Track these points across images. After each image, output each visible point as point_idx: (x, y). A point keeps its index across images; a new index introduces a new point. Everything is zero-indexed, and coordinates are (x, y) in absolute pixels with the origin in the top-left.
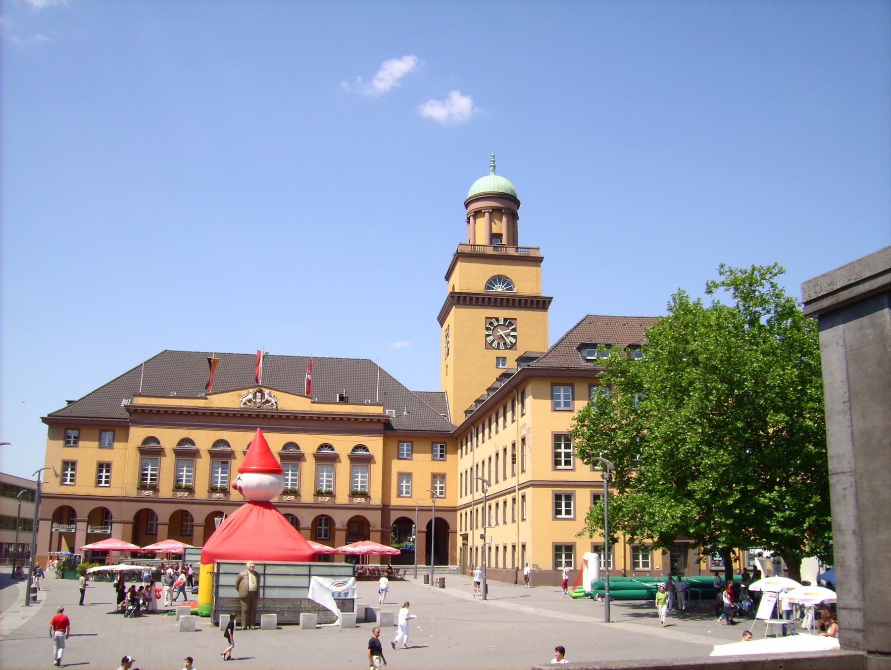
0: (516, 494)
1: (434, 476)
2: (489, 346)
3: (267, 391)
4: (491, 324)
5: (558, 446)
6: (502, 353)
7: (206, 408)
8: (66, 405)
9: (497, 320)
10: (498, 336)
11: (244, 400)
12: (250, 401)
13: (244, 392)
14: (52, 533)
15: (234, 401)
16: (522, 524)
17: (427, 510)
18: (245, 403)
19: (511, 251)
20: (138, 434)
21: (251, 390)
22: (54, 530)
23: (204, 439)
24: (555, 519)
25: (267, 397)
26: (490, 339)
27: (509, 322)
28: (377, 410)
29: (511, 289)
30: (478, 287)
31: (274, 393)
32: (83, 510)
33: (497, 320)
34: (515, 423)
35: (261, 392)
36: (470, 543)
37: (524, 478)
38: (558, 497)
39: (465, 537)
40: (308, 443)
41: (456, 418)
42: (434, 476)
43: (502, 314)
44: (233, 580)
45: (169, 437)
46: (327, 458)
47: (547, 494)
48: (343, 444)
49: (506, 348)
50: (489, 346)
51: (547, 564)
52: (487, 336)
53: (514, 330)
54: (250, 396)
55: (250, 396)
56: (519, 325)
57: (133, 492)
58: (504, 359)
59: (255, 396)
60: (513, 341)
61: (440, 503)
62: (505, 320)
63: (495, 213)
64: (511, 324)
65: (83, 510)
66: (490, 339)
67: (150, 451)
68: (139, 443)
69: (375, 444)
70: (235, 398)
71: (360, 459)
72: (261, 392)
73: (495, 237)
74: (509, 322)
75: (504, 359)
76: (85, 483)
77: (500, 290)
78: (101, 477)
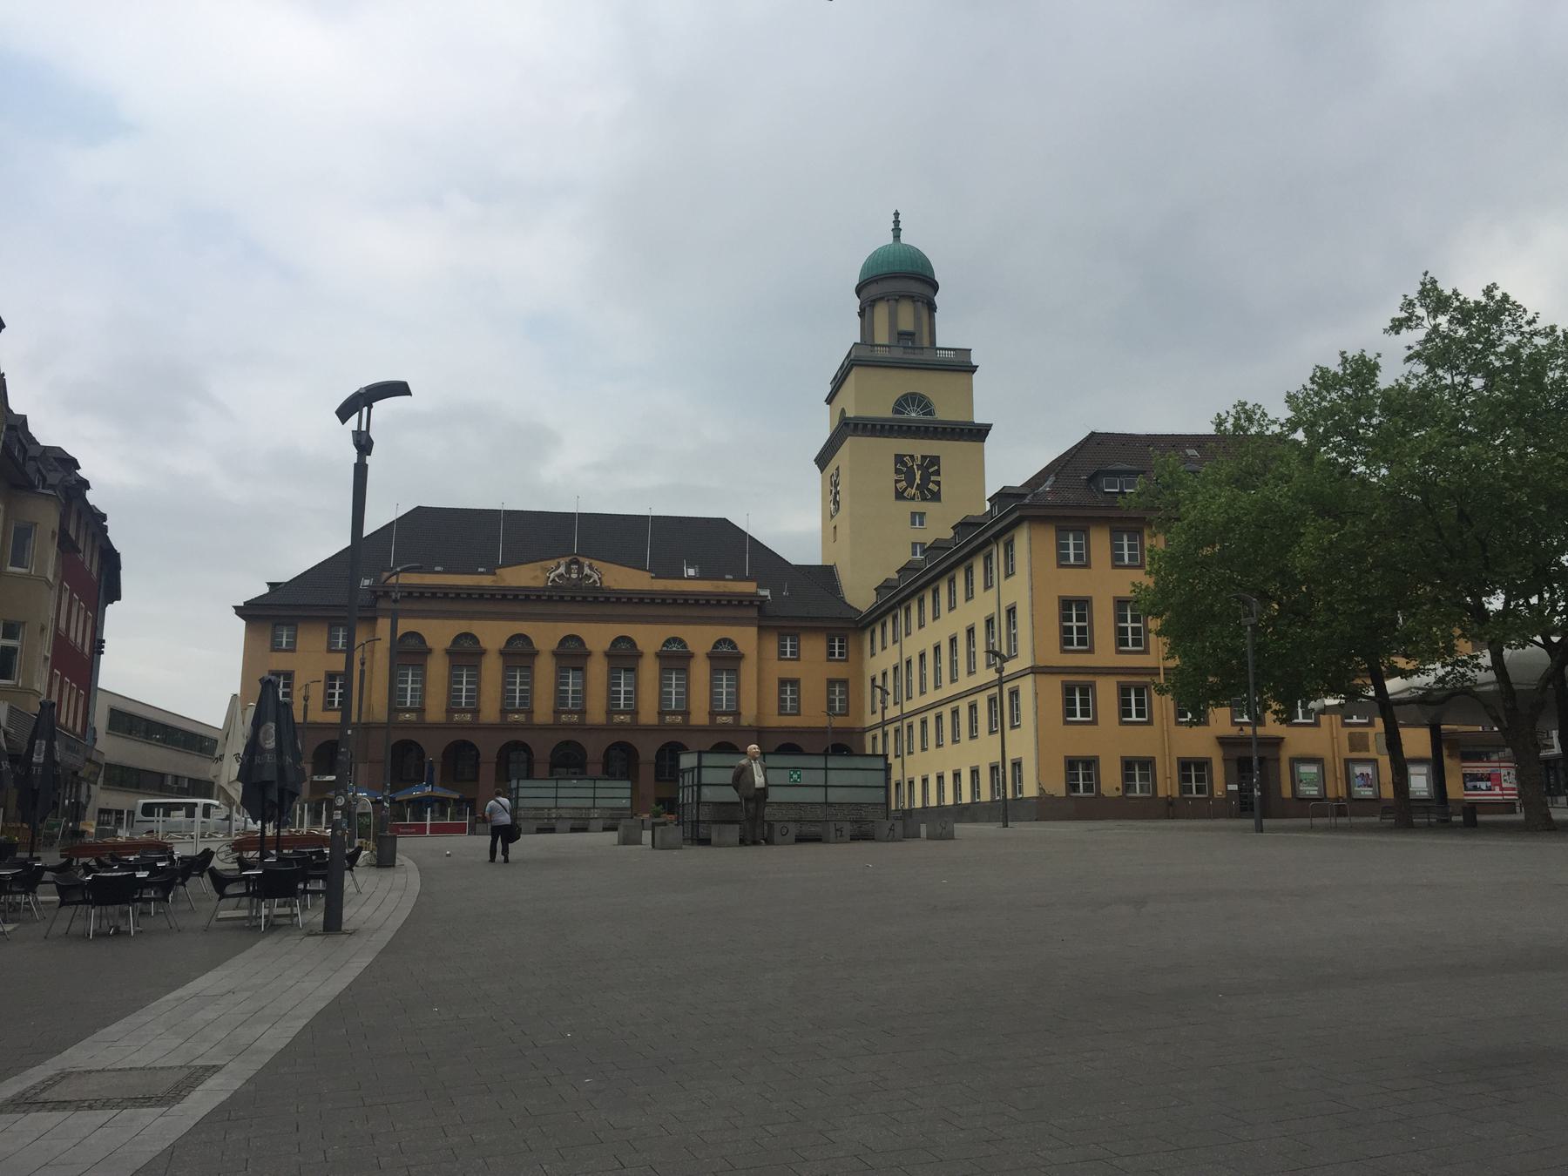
2: (900, 495)
6: (919, 506)
8: (266, 590)
10: (919, 481)
12: (560, 576)
13: (552, 563)
15: (536, 577)
17: (822, 731)
21: (562, 561)
24: (1067, 723)
25: (587, 571)
27: (931, 464)
28: (749, 587)
29: (931, 413)
31: (596, 564)
33: (912, 457)
35: (577, 562)
36: (896, 775)
38: (1068, 690)
40: (649, 637)
45: (439, 633)
46: (675, 659)
47: (1055, 684)
48: (700, 638)
49: (924, 499)
50: (900, 495)
51: (1058, 788)
54: (562, 570)
55: (562, 570)
58: (922, 515)
59: (568, 570)
61: (839, 722)
67: (410, 653)
69: (745, 637)
70: (539, 573)
72: (577, 562)
75: (922, 515)
78: (333, 695)
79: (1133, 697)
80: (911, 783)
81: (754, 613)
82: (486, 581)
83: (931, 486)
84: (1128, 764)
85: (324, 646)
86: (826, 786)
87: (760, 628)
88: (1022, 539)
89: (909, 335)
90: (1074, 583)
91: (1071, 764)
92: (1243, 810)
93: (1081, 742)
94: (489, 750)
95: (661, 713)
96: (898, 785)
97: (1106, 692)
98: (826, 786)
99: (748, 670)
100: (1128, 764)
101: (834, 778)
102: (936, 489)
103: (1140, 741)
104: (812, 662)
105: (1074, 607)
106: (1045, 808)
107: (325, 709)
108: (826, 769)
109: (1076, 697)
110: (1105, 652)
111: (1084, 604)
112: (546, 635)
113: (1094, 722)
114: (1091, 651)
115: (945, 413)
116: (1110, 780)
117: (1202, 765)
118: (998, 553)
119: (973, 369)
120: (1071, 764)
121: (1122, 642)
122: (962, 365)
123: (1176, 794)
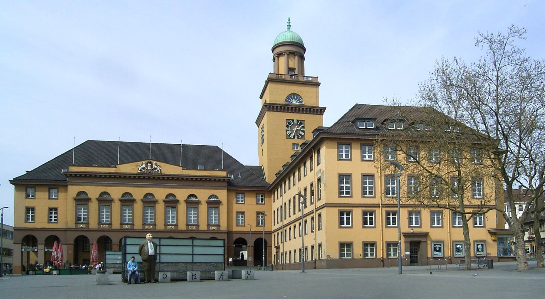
0: (314, 214)
1: (258, 213)
2: (288, 137)
3: (154, 163)
4: (289, 123)
5: (341, 182)
7: (116, 173)
9: (293, 121)
11: (140, 168)
13: (140, 163)
14: (22, 252)
16: (319, 233)
18: (141, 170)
19: (301, 79)
20: (73, 190)
22: (23, 250)
23: (116, 192)
25: (154, 166)
26: (289, 132)
27: (300, 123)
28: (223, 174)
30: (281, 100)
31: (159, 163)
32: (41, 238)
34: (313, 171)
35: (150, 163)
36: (281, 251)
37: (319, 204)
38: (342, 214)
39: (278, 248)
40: (181, 194)
41: (269, 178)
42: (258, 213)
43: (296, 117)
44: (136, 249)
45: (93, 191)
47: (335, 211)
48: (203, 194)
49: (298, 138)
50: (288, 137)
51: (335, 255)
52: (287, 130)
53: (303, 127)
54: (144, 166)
55: (144, 166)
56: (306, 124)
57: (72, 225)
59: (147, 166)
60: (303, 134)
61: (260, 229)
62: (298, 121)
63: (291, 53)
64: (301, 124)
65: (41, 238)
66: (289, 132)
67: (82, 200)
68: (75, 196)
69: (222, 194)
70: (135, 167)
71: (214, 204)
72: (150, 163)
73: (291, 70)
74: (300, 123)
76: (41, 221)
77: (294, 103)
78: (51, 217)
79: (368, 217)
80: (286, 253)
81: (225, 184)
82: (112, 170)
83: (301, 133)
84: (366, 244)
85: (47, 197)
86: (193, 254)
87: (228, 190)
88: (323, 150)
89: (293, 69)
90: (345, 168)
91: (342, 245)
92: (411, 262)
93: (346, 235)
94: (93, 239)
95: (187, 225)
96: (282, 254)
97: (357, 214)
98: (193, 254)
99: (223, 208)
100: (366, 244)
101: (197, 250)
102: (303, 134)
103: (370, 235)
104: (249, 204)
105: (344, 177)
106: (331, 264)
107: (49, 223)
108: (193, 246)
109: (344, 216)
110: (357, 198)
111: (349, 176)
112: (138, 193)
113: (352, 227)
114: (351, 197)
115: (307, 102)
116: (358, 251)
117: (395, 244)
118: (315, 156)
119: (318, 84)
120: (342, 245)
121: (364, 193)
122: (314, 84)
123: (385, 257)
